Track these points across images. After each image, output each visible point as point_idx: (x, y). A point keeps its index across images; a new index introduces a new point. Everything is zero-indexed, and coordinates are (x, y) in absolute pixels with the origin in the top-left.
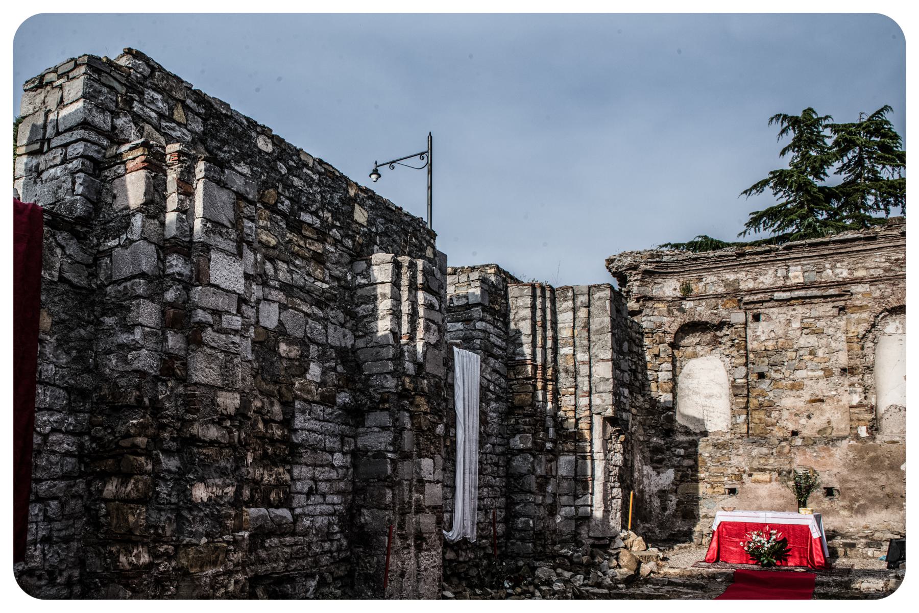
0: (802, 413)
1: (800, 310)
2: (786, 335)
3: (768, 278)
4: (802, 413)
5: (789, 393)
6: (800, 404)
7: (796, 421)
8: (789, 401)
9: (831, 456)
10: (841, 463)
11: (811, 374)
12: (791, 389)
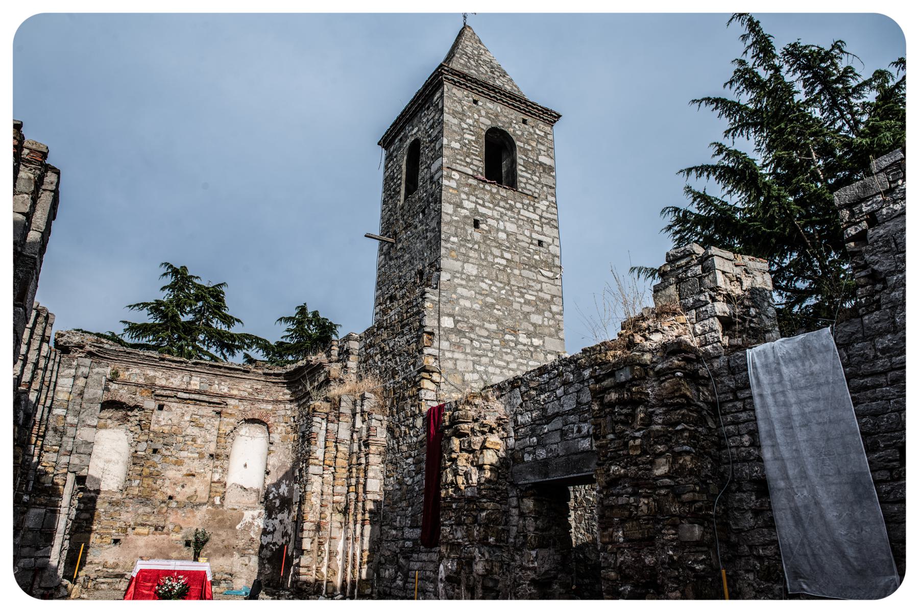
0: (179, 483)
1: (192, 408)
2: (179, 424)
3: (177, 380)
4: (179, 483)
5: (173, 467)
6: (179, 476)
7: (174, 489)
8: (172, 473)
9: (194, 516)
10: (200, 522)
11: (190, 455)
12: (175, 465)
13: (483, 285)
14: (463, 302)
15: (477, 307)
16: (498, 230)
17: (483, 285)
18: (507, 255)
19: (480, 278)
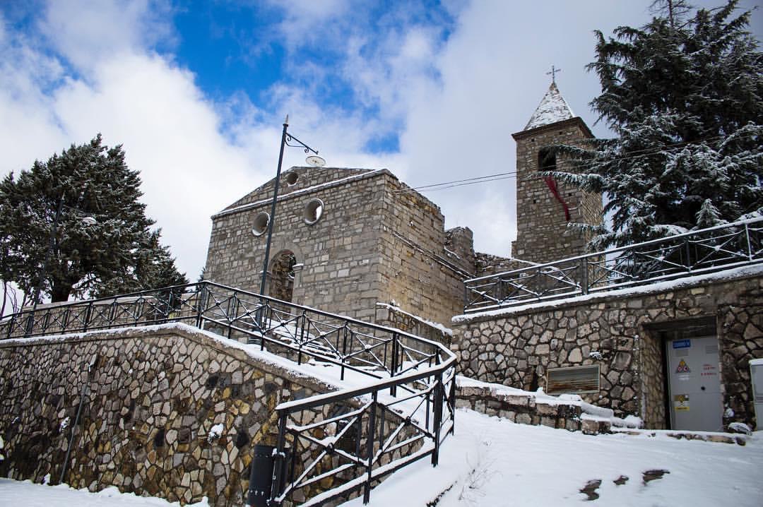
13: (538, 229)
14: (528, 241)
15: (535, 240)
16: (545, 199)
17: (538, 229)
18: (550, 210)
19: (537, 226)
